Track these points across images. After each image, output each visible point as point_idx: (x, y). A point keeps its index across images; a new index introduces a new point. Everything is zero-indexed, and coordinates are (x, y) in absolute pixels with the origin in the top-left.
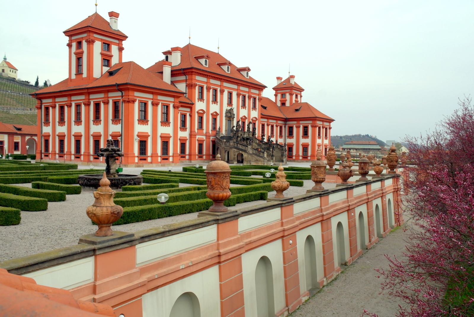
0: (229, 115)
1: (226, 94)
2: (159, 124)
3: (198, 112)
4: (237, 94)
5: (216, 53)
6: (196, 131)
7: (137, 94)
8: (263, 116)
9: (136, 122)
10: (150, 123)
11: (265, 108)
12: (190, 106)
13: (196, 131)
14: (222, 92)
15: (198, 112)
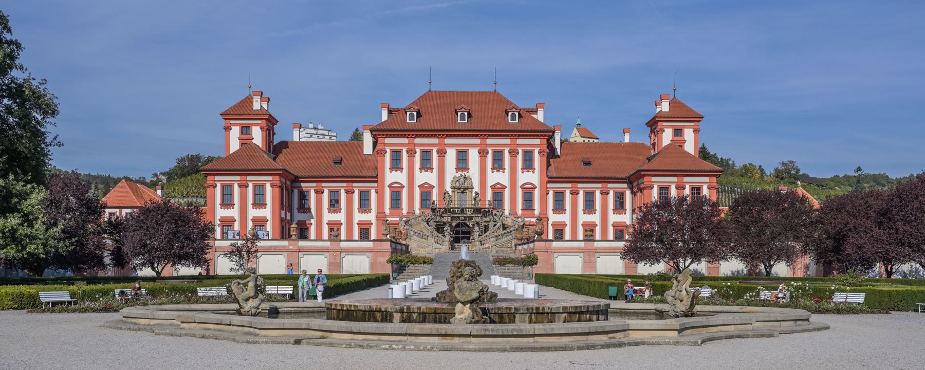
0: (457, 184)
1: (451, 154)
2: (250, 206)
3: (390, 186)
4: (479, 152)
5: (489, 93)
6: (387, 212)
7: (217, 178)
8: (552, 180)
9: (218, 206)
10: (237, 206)
11: (587, 164)
12: (375, 178)
13: (387, 212)
14: (442, 153)
15: (390, 186)
